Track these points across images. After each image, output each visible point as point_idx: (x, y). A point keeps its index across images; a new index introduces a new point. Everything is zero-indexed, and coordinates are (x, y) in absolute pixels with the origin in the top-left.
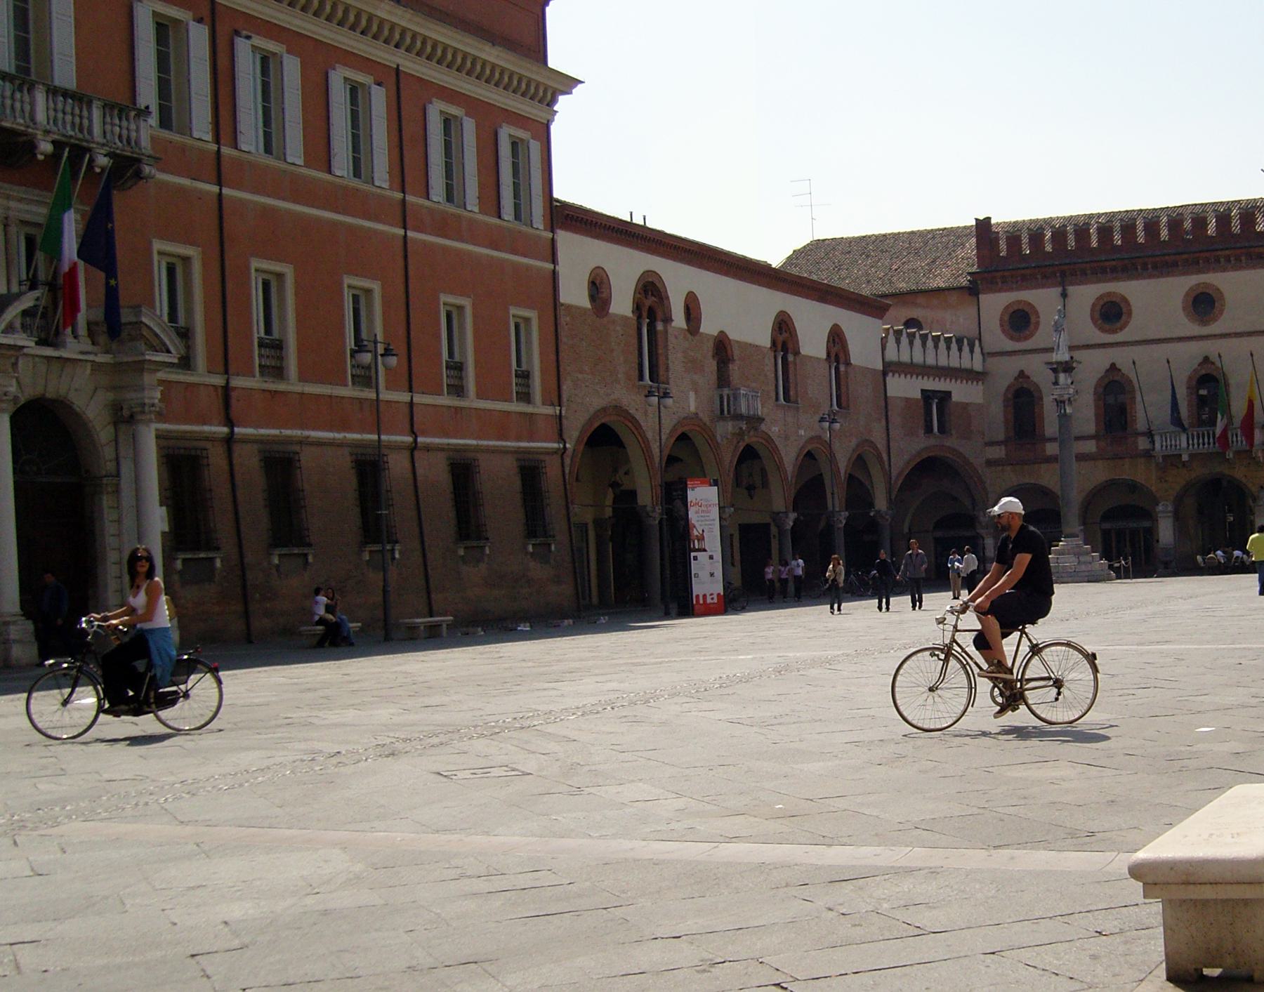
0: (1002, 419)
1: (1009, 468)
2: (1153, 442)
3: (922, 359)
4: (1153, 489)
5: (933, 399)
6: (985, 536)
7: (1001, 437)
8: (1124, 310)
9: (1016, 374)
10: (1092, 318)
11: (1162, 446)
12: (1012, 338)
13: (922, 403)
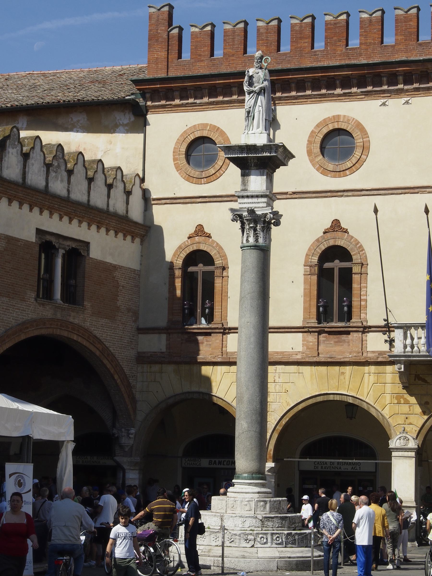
0: (167, 295)
1: (170, 368)
2: (391, 342)
3: (44, 183)
4: (386, 413)
5: (57, 250)
6: (125, 467)
7: (163, 322)
8: (359, 141)
9: (192, 230)
10: (309, 153)
11: (405, 347)
12: (189, 178)
13: (37, 249)
